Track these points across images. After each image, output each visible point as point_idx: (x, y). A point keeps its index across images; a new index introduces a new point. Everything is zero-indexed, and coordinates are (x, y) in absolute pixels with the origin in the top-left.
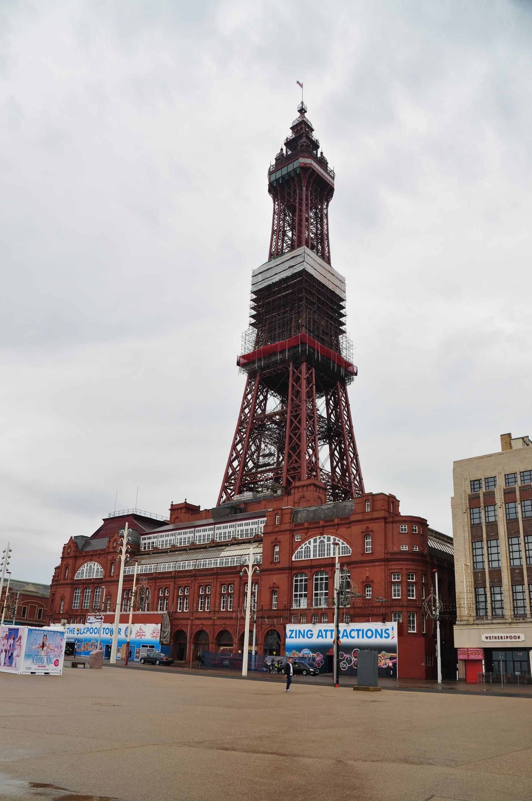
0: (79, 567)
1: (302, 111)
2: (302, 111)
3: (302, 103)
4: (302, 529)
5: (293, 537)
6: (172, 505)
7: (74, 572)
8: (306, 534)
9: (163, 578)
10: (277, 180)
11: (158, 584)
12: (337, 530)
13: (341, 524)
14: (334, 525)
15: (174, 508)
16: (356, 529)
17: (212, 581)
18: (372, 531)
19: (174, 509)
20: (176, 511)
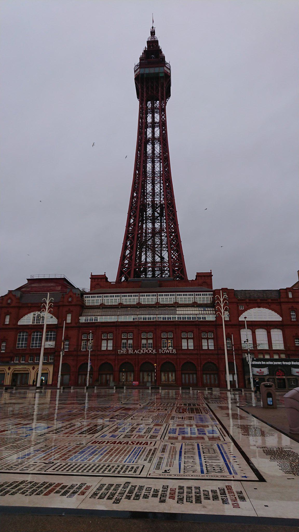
0: (24, 315)
1: (153, 33)
2: (153, 33)
3: (153, 28)
4: (255, 303)
5: (238, 306)
6: (91, 275)
7: (19, 319)
8: (248, 306)
9: (127, 326)
10: (143, 75)
11: (121, 330)
12: (270, 306)
13: (273, 303)
14: (268, 303)
15: (94, 277)
16: (284, 306)
17: (174, 329)
18: (296, 309)
19: (94, 278)
20: (96, 280)
